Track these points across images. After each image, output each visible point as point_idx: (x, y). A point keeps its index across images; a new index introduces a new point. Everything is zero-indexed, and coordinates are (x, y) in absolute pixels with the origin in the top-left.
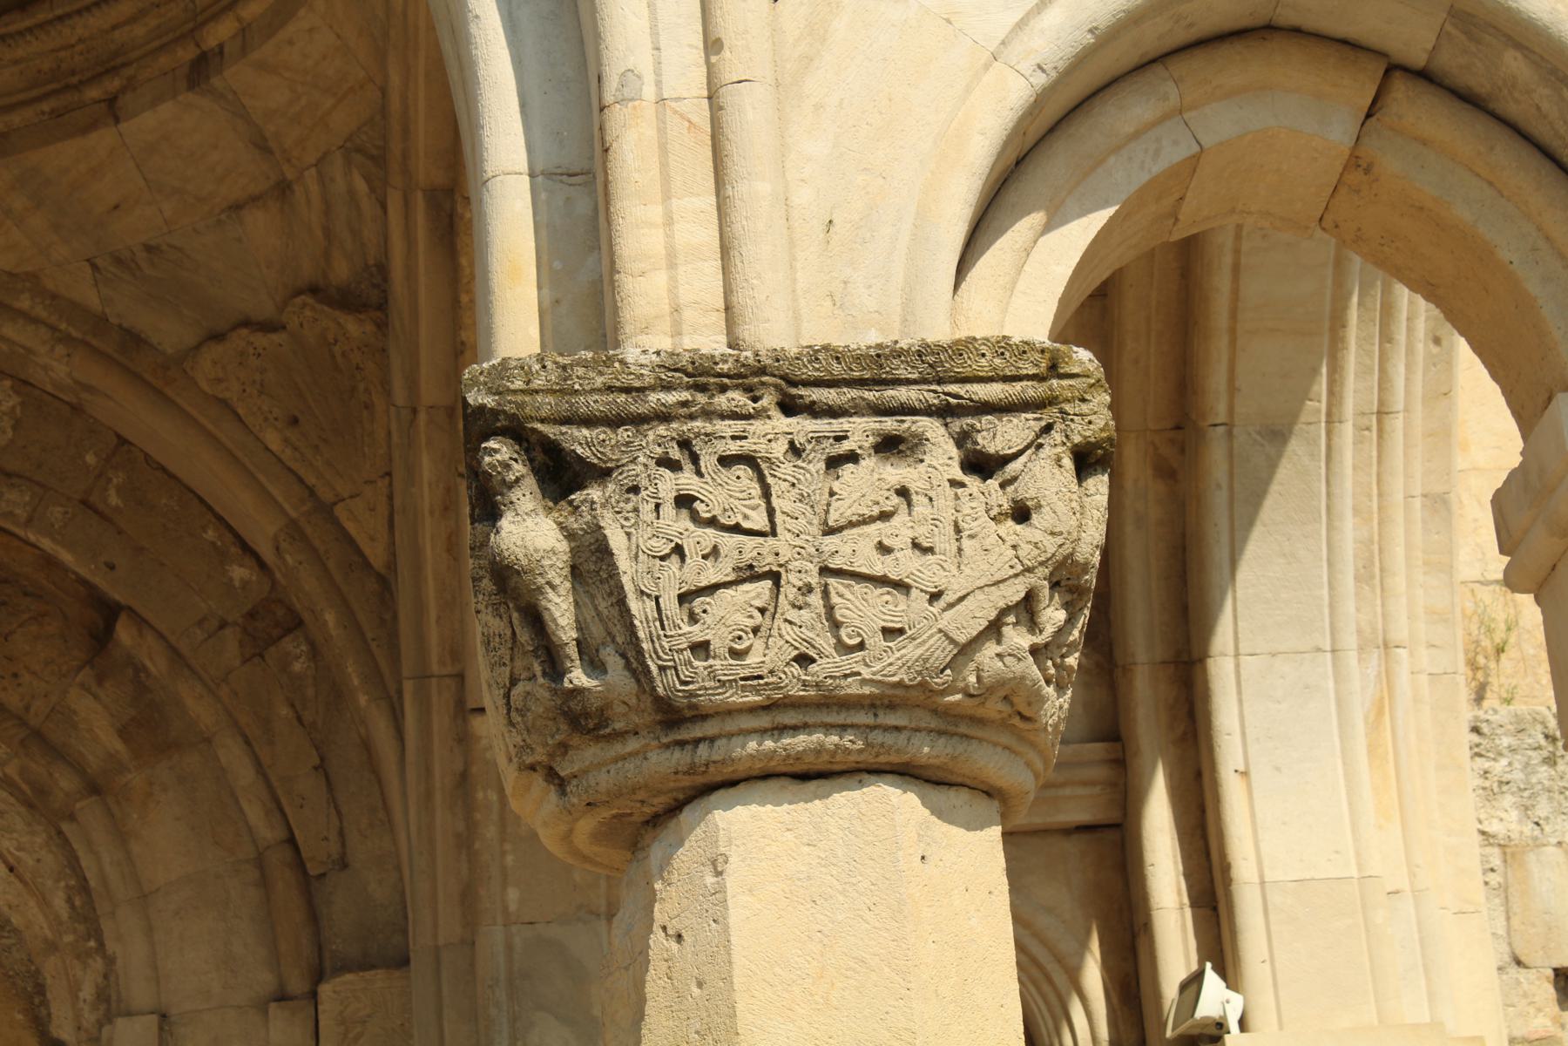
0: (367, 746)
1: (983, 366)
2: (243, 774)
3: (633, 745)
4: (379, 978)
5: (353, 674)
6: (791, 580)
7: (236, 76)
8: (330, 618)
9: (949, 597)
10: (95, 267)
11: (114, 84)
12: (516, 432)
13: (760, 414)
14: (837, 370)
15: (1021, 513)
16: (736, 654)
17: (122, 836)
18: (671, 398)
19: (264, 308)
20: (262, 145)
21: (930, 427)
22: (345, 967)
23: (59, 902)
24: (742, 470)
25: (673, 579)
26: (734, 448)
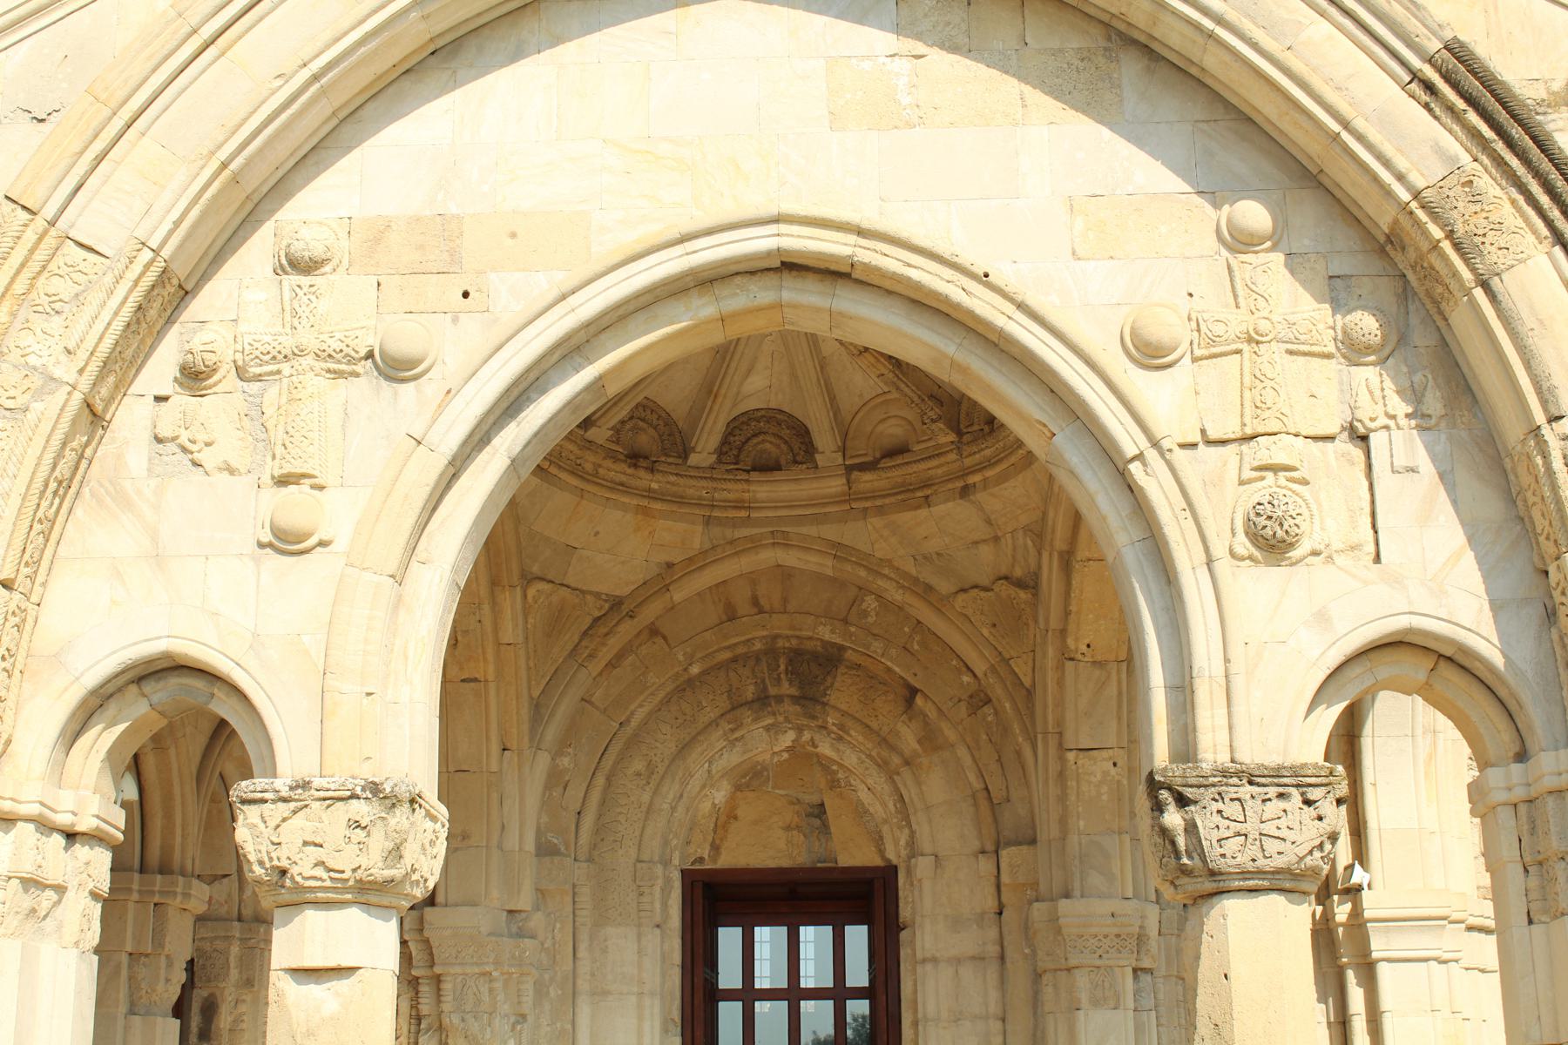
0: (1019, 753)
1: (1309, 772)
2: (967, 761)
3: (1200, 880)
4: (1024, 848)
5: (1016, 728)
6: (1251, 837)
7: (980, 496)
8: (1007, 705)
9: (1298, 843)
10: (915, 559)
11: (929, 492)
12: (1170, 789)
13: (1242, 785)
14: (1266, 772)
15: (1320, 818)
16: (1233, 858)
17: (919, 783)
18: (1216, 780)
19: (985, 582)
20: (989, 522)
21: (1293, 791)
22: (1009, 844)
23: (891, 805)
24: (1237, 803)
25: (1215, 835)
26: (1235, 796)
